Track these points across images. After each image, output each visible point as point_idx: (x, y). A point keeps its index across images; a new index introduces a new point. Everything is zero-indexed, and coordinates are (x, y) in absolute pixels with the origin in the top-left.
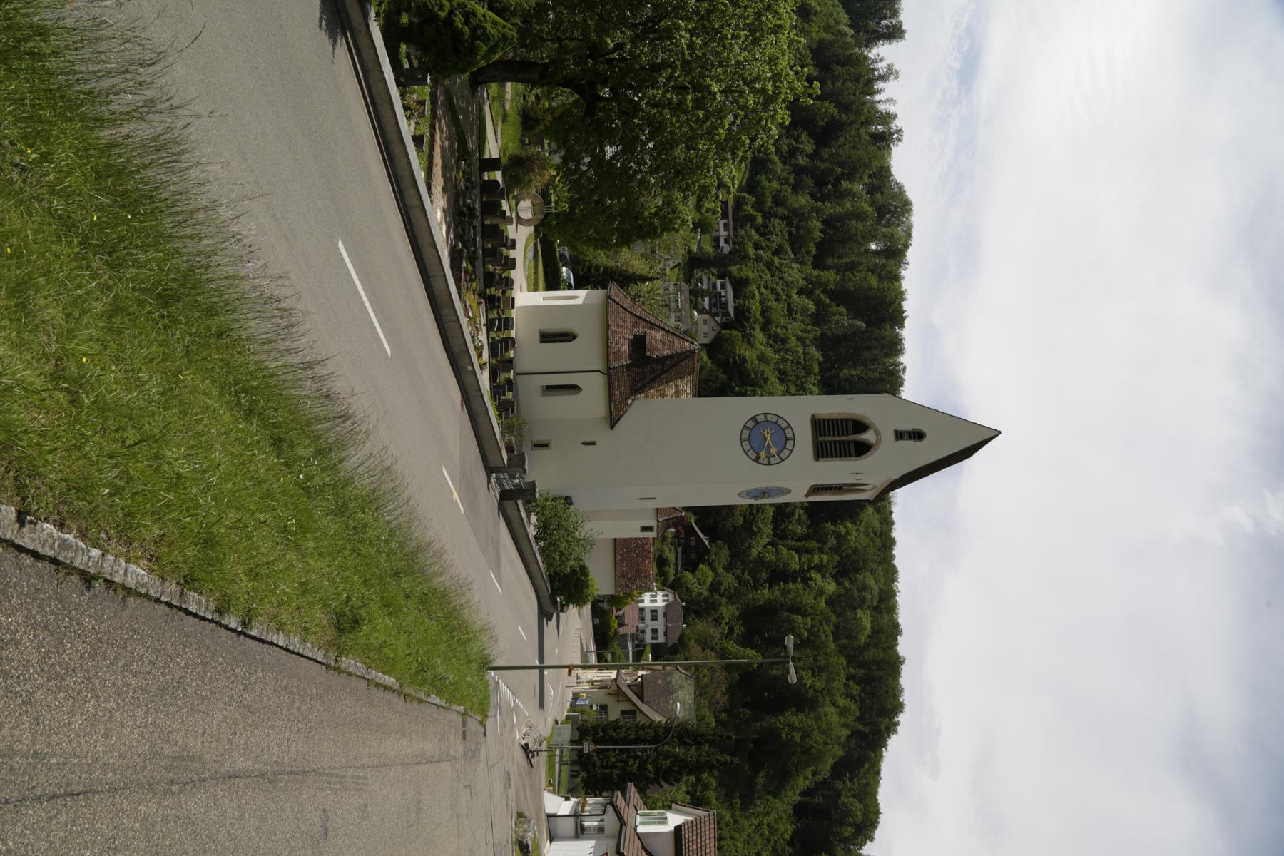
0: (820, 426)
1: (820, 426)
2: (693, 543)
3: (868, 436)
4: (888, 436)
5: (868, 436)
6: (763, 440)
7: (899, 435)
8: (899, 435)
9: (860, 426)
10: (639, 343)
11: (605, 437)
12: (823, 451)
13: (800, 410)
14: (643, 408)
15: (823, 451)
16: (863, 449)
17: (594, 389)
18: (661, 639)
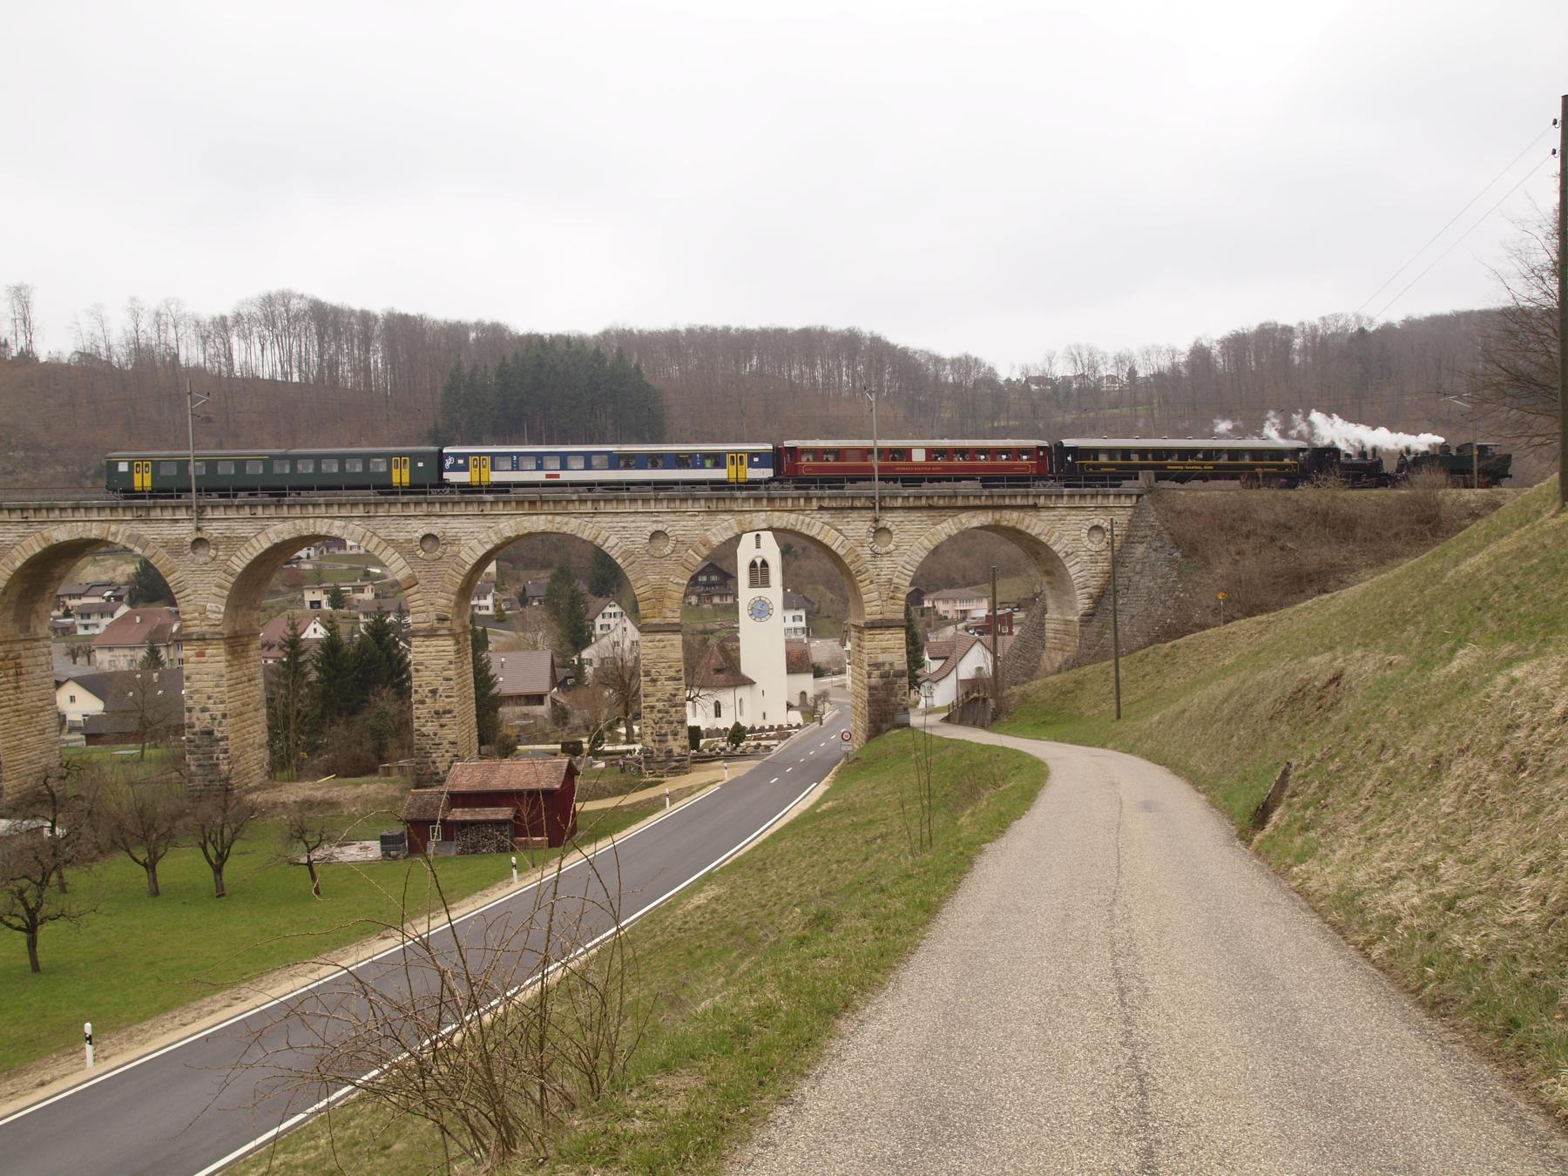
0: (753, 584)
1: (753, 584)
2: (704, 579)
3: (759, 562)
4: (758, 552)
5: (759, 562)
6: (760, 610)
7: (758, 546)
8: (758, 546)
9: (753, 564)
10: (719, 671)
11: (759, 687)
12: (765, 583)
13: (746, 594)
14: (746, 669)
15: (765, 583)
16: (764, 563)
17: (742, 692)
18: (802, 613)
